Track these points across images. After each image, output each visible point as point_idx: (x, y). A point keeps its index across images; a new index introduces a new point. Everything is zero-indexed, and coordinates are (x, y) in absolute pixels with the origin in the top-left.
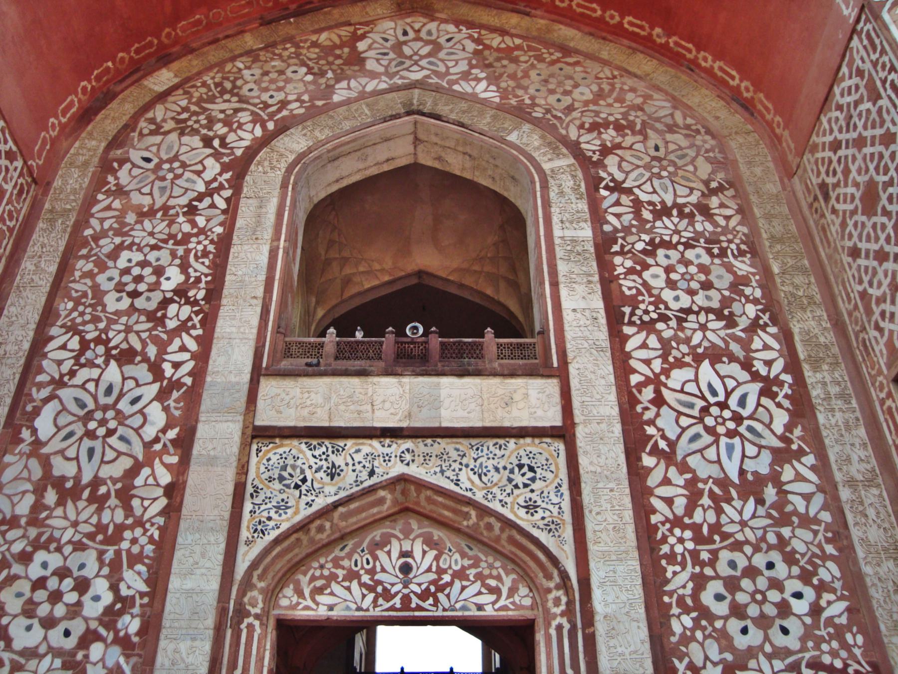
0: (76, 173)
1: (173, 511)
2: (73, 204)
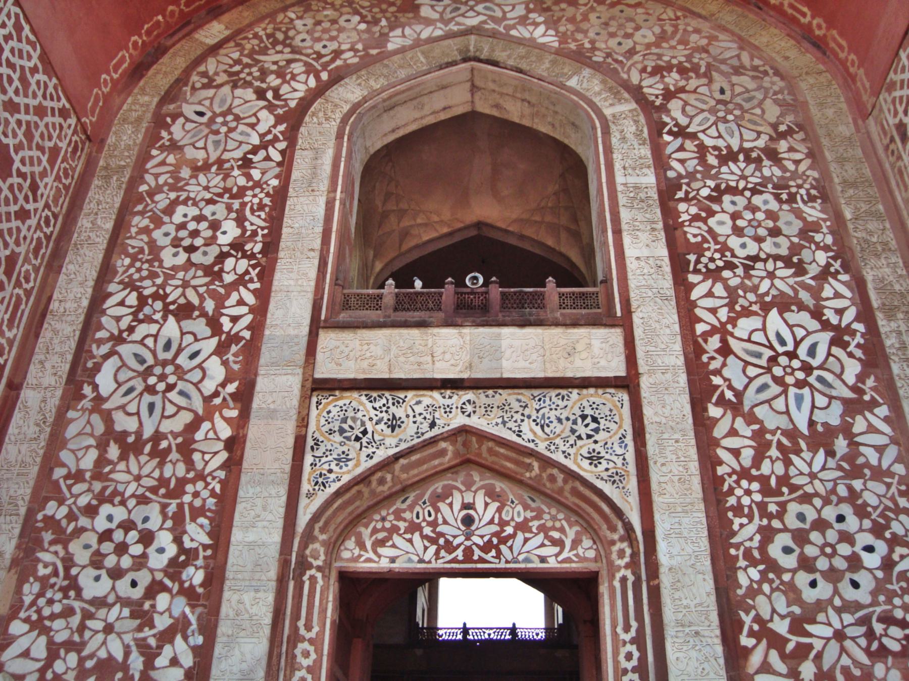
0: (129, 129)
1: (234, 464)
2: (127, 160)
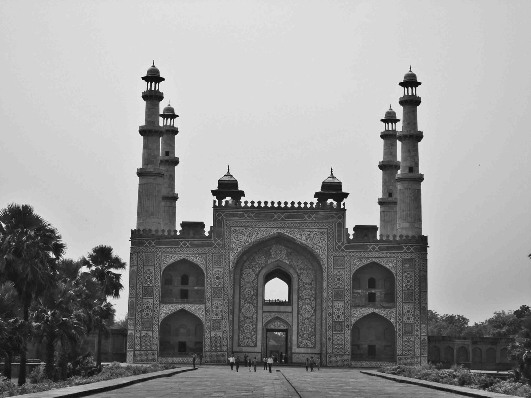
1: (257, 320)
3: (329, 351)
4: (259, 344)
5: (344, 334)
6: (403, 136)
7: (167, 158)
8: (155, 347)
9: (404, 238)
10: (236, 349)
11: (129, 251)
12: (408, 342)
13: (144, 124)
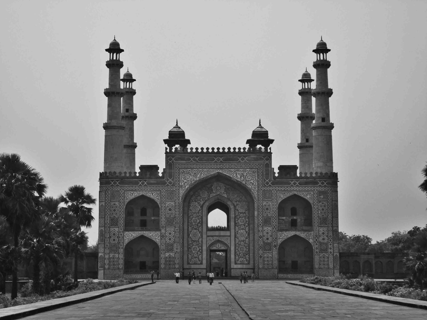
3: (261, 266)
4: (204, 262)
5: (272, 252)
6: (317, 92)
7: (127, 114)
8: (121, 266)
9: (319, 175)
10: (186, 266)
11: (99, 190)
12: (324, 257)
13: (108, 87)
